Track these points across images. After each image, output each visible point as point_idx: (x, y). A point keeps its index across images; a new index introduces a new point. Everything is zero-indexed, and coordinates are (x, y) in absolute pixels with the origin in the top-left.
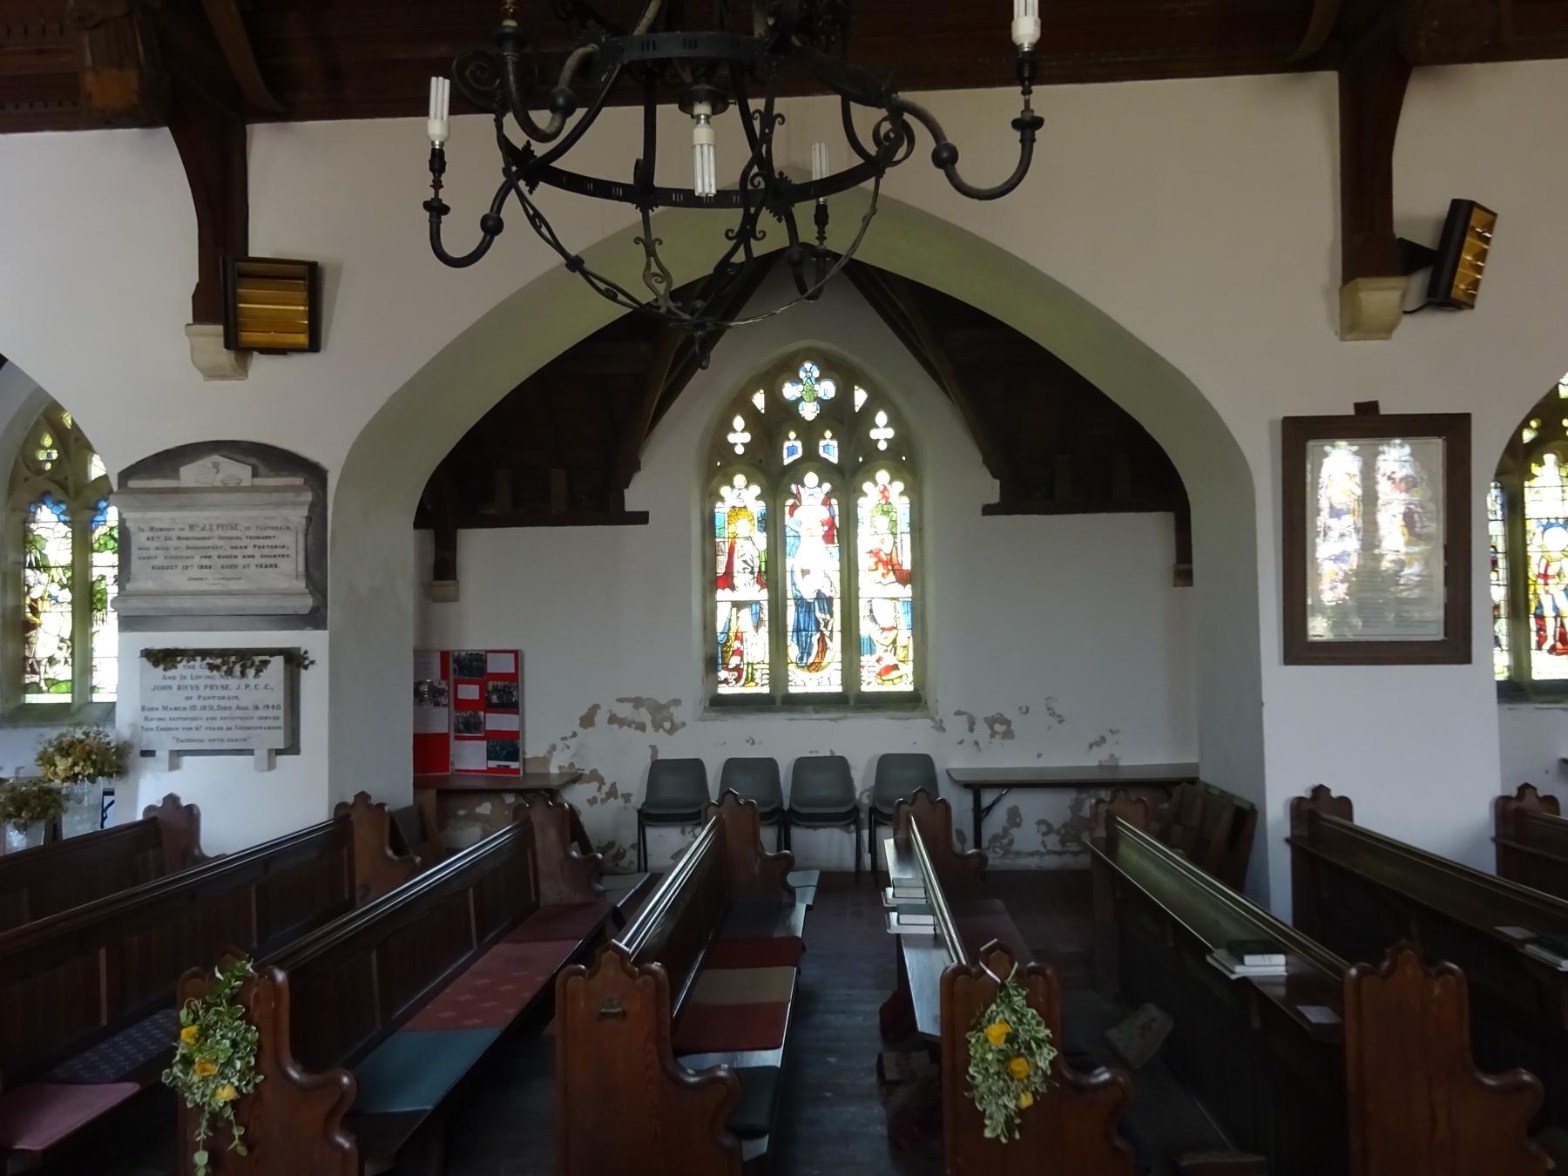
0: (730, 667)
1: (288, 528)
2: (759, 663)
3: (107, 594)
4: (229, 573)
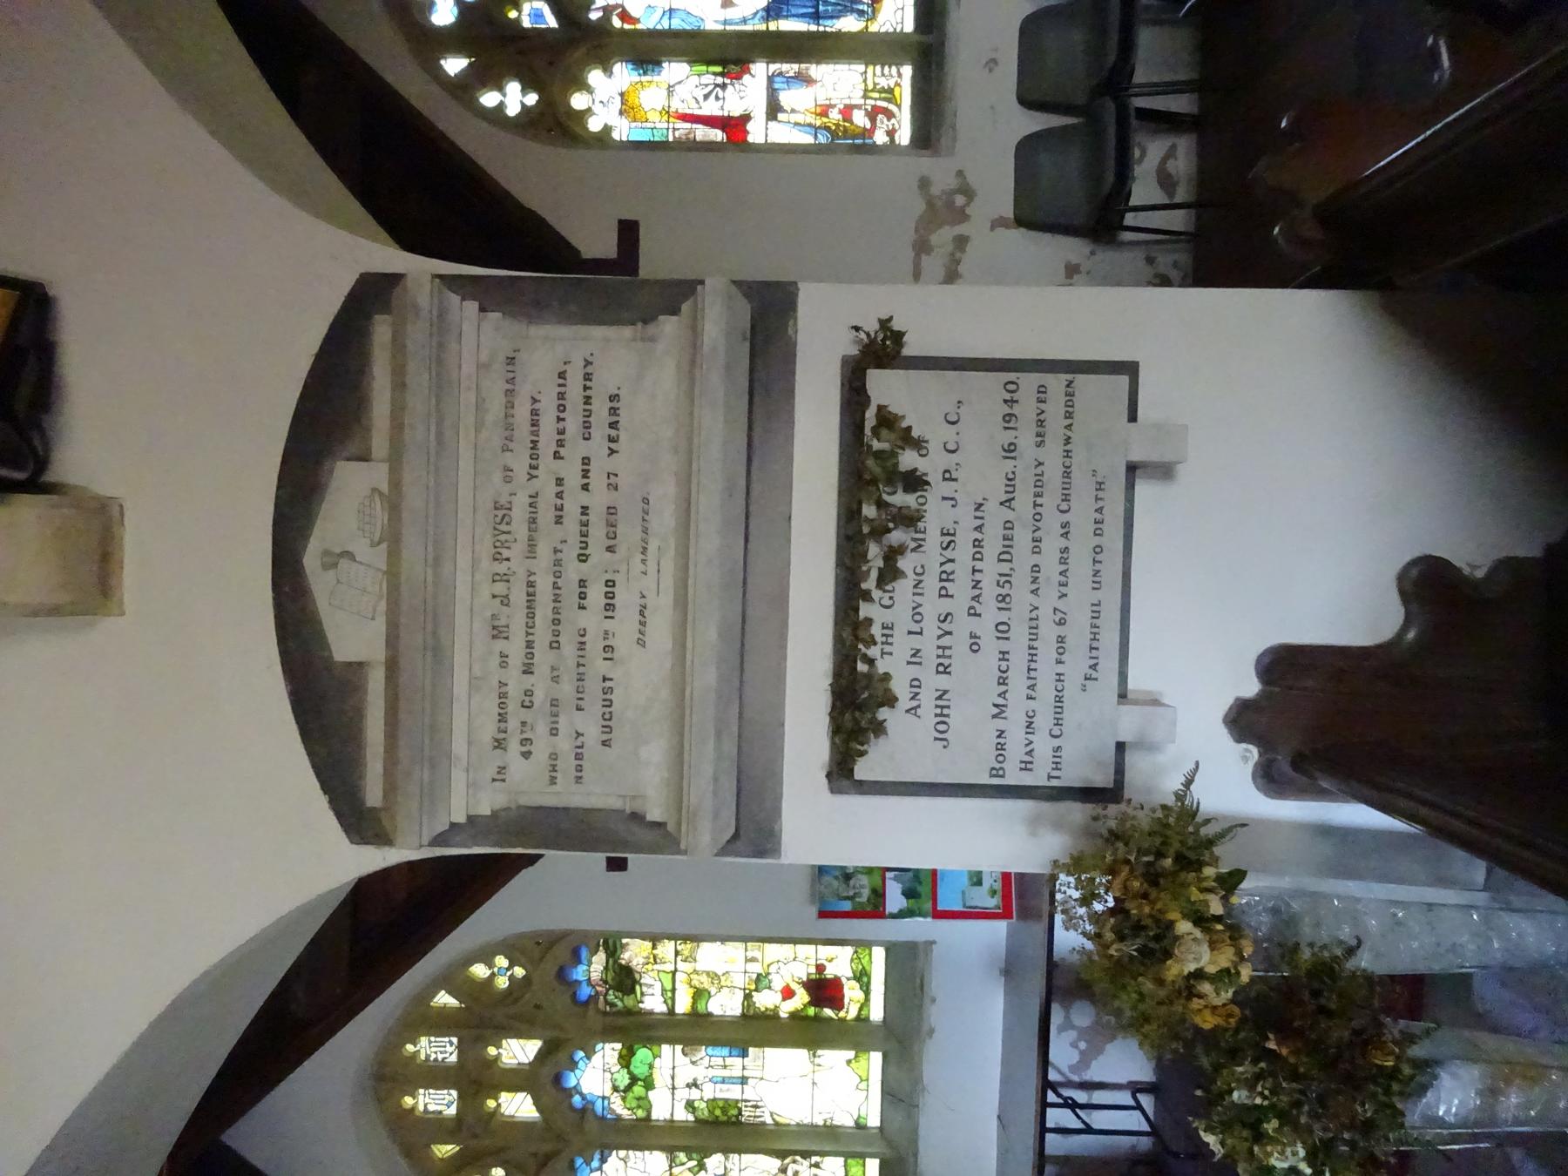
0: (868, 126)
1: (511, 360)
2: (865, 81)
3: (715, 1100)
4: (628, 532)
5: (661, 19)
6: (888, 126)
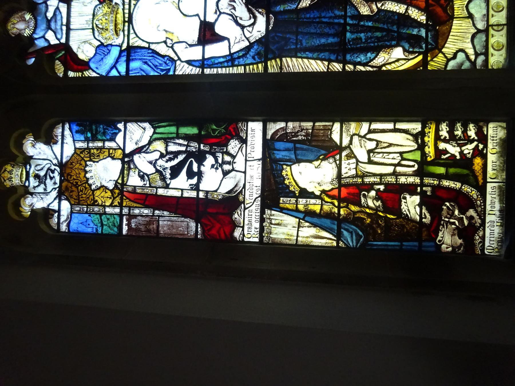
2: (422, 147)
6: (461, 220)
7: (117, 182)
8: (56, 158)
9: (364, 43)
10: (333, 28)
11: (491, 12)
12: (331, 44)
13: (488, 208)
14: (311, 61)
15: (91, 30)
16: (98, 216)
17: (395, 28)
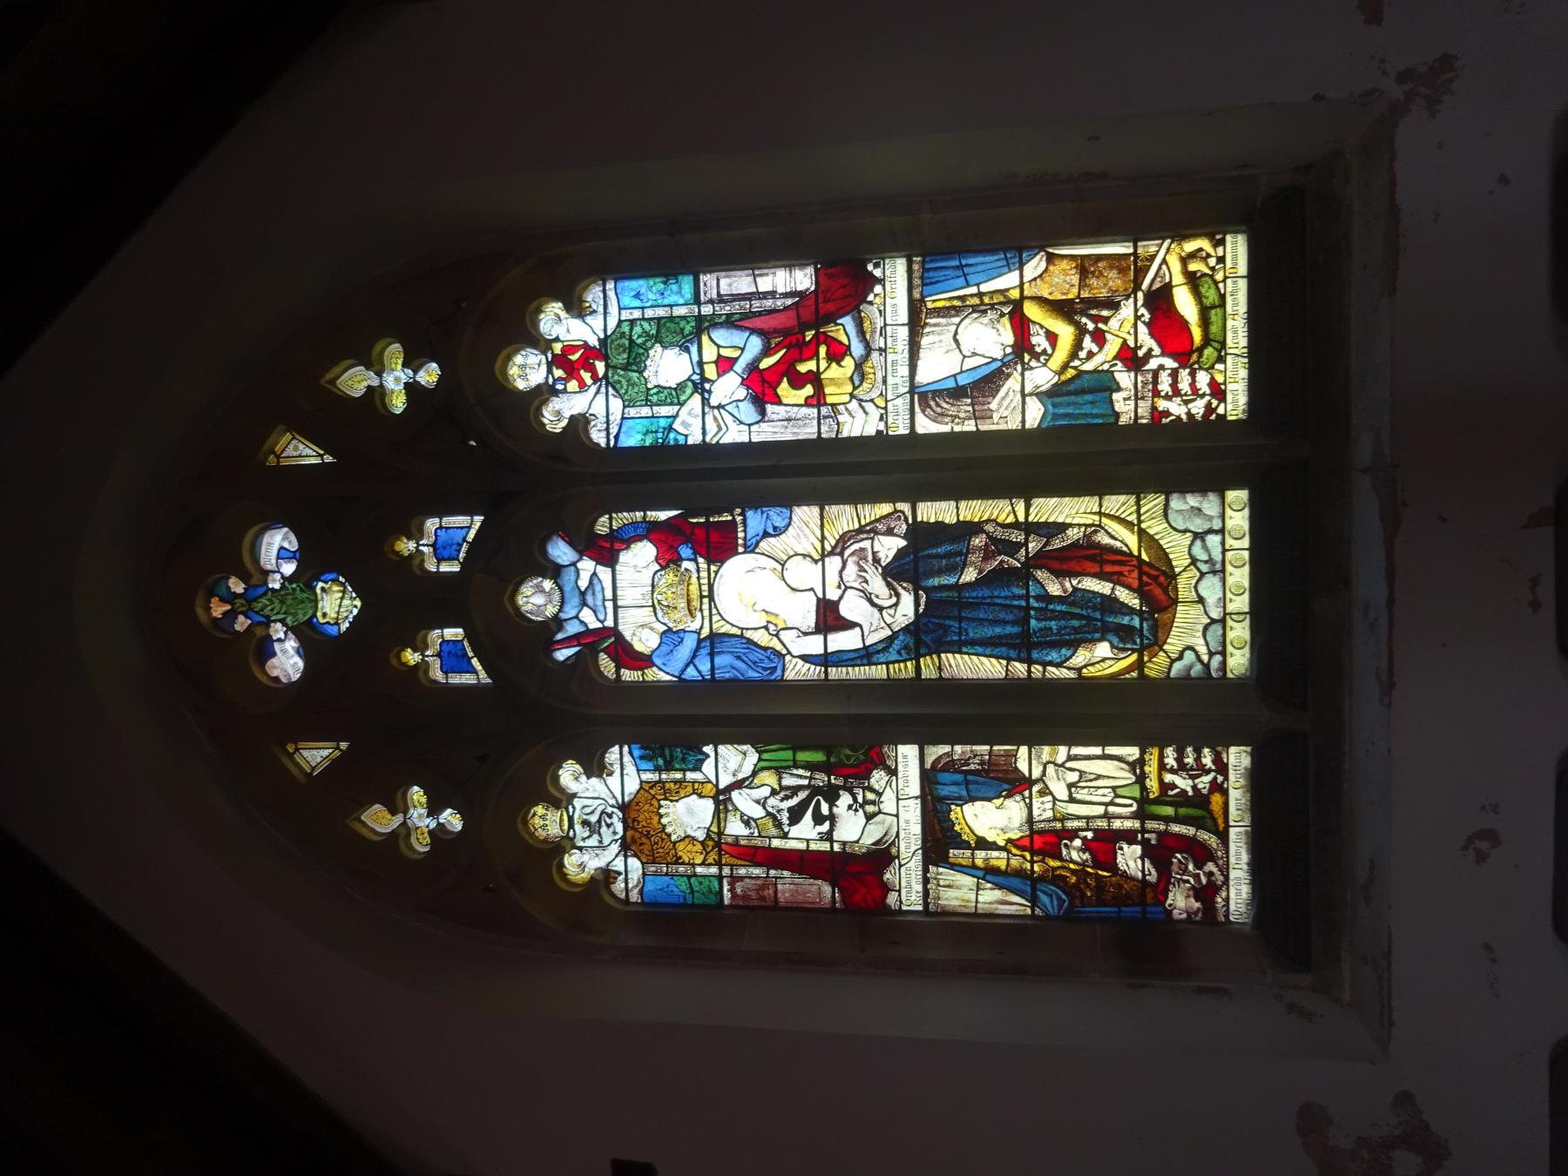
2: (1141, 779)
5: (694, 656)
6: (1197, 877)
7: (709, 829)
8: (614, 797)
9: (1056, 635)
10: (1011, 612)
11: (1229, 595)
12: (1011, 636)
13: (1232, 860)
14: (982, 658)
15: (651, 609)
16: (685, 879)
17: (1098, 615)
